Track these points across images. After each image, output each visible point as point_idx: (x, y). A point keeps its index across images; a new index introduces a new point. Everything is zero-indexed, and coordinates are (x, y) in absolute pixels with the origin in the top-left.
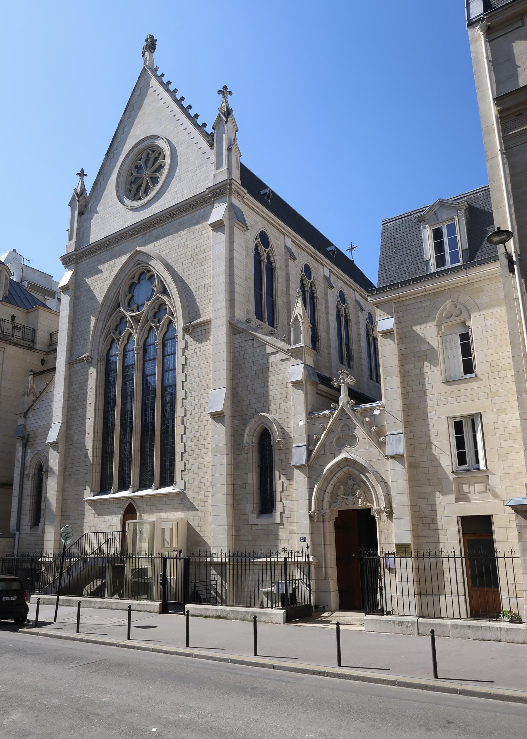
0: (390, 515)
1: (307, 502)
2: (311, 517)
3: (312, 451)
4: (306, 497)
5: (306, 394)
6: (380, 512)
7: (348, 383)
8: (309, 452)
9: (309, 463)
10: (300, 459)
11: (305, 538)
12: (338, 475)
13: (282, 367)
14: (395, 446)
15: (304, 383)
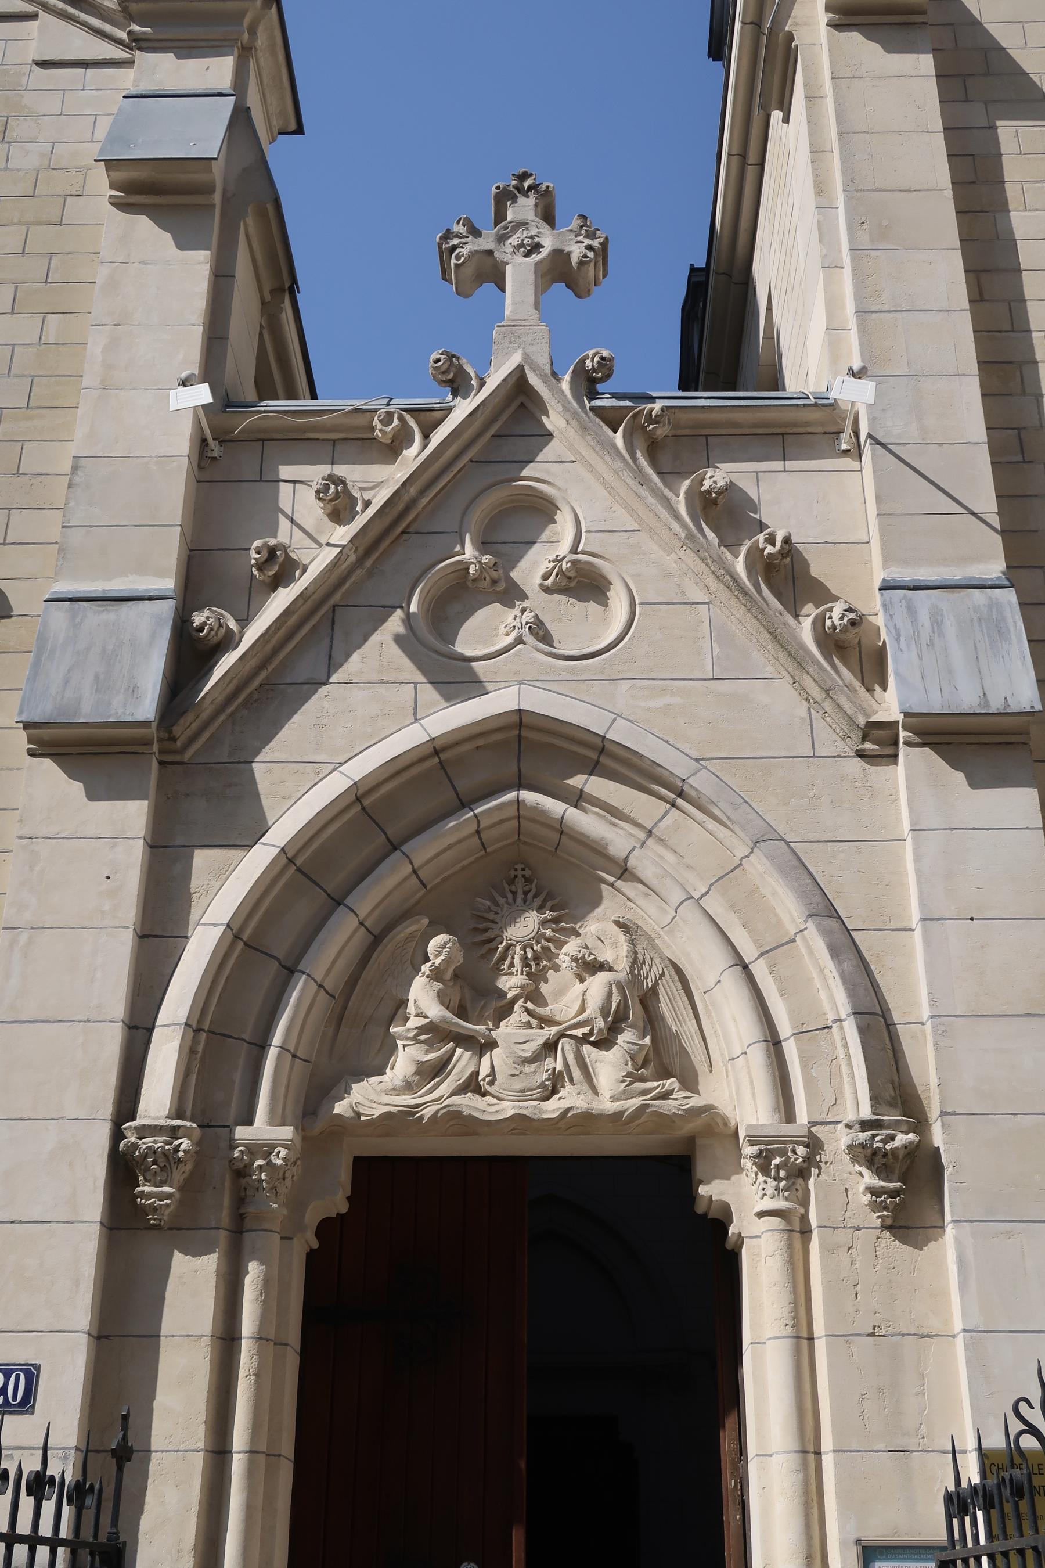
0: (911, 1188)
1: (111, 1041)
2: (123, 1170)
3: (228, 642)
4: (115, 1002)
5: (221, 278)
6: (794, 1165)
7: (560, 256)
8: (191, 654)
9: (182, 730)
10: (101, 685)
11: (32, 1374)
12: (424, 850)
13: (51, 104)
14: (958, 655)
15: (217, 198)
